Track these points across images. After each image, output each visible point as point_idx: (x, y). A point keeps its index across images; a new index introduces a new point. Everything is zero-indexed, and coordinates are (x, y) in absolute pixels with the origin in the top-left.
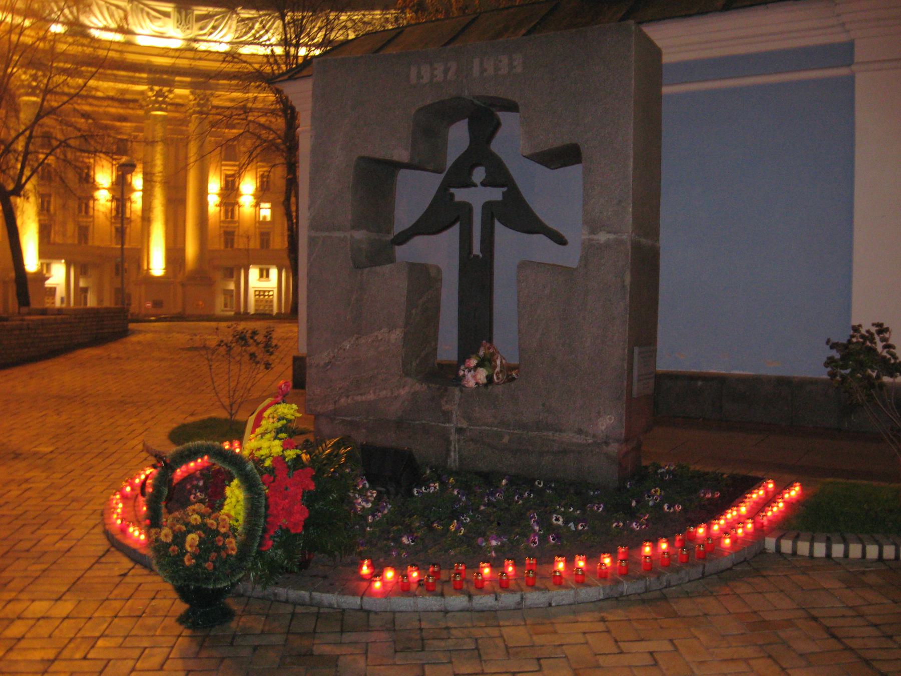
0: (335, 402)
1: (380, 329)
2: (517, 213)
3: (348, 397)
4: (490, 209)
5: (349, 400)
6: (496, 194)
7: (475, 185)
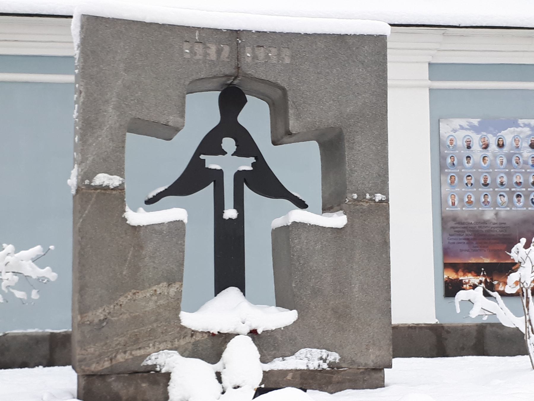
0: (111, 360)
1: (159, 284)
2: (263, 180)
3: (125, 352)
7: (224, 153)
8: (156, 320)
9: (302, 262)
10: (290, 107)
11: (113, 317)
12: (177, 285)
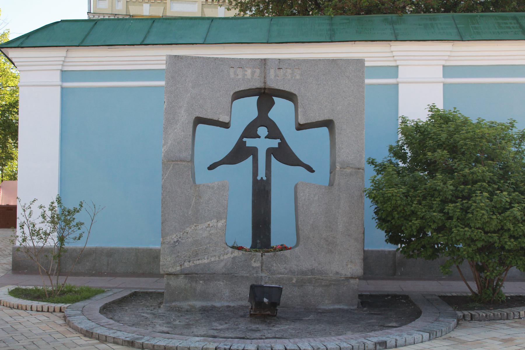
0: (181, 266)
1: (211, 220)
2: (284, 154)
3: (189, 262)
4: (270, 152)
5: (191, 264)
6: (274, 143)
7: (259, 137)
8: (209, 243)
9: (305, 208)
10: (299, 107)
11: (182, 240)
12: (223, 221)
